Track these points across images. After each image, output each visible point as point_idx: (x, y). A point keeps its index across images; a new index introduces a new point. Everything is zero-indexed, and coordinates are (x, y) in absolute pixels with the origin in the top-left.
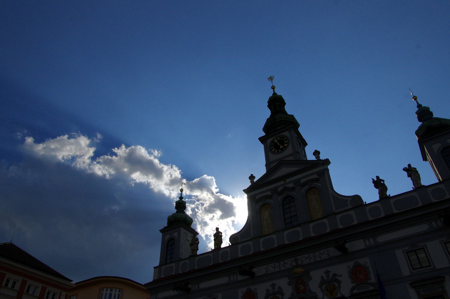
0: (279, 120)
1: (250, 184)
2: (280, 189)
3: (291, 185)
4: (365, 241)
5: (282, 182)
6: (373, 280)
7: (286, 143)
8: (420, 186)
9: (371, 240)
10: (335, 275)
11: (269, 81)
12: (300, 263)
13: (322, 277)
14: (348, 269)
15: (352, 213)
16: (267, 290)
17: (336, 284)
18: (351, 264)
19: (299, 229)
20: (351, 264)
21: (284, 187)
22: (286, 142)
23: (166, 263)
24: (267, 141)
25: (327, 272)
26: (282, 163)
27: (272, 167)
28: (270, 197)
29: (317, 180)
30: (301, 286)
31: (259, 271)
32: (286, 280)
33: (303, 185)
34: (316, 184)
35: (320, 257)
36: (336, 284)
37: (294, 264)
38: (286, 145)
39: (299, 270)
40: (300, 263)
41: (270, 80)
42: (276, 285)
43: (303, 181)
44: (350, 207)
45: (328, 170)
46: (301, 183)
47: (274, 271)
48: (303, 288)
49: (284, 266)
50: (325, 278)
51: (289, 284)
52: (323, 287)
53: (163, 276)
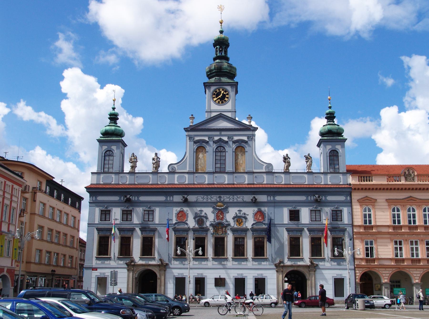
0: (224, 71)
2: (216, 138)
3: (225, 139)
4: (268, 197)
5: (218, 133)
6: (266, 222)
7: (227, 98)
8: (310, 171)
9: (272, 197)
10: (245, 214)
11: (219, 10)
12: (222, 200)
13: (236, 213)
14: (254, 211)
16: (196, 213)
18: (256, 209)
20: (256, 209)
21: (220, 138)
22: (227, 96)
24: (210, 88)
25: (240, 211)
26: (221, 116)
27: (212, 116)
28: (207, 142)
29: (246, 142)
30: (220, 215)
31: (192, 198)
32: (211, 209)
34: (244, 144)
35: (237, 199)
36: (244, 220)
37: (218, 200)
38: (226, 99)
40: (222, 200)
41: (220, 9)
43: (236, 138)
45: (254, 135)
46: (233, 140)
47: (202, 201)
48: (221, 217)
49: (211, 199)
50: (238, 214)
51: (213, 212)
52: (235, 219)
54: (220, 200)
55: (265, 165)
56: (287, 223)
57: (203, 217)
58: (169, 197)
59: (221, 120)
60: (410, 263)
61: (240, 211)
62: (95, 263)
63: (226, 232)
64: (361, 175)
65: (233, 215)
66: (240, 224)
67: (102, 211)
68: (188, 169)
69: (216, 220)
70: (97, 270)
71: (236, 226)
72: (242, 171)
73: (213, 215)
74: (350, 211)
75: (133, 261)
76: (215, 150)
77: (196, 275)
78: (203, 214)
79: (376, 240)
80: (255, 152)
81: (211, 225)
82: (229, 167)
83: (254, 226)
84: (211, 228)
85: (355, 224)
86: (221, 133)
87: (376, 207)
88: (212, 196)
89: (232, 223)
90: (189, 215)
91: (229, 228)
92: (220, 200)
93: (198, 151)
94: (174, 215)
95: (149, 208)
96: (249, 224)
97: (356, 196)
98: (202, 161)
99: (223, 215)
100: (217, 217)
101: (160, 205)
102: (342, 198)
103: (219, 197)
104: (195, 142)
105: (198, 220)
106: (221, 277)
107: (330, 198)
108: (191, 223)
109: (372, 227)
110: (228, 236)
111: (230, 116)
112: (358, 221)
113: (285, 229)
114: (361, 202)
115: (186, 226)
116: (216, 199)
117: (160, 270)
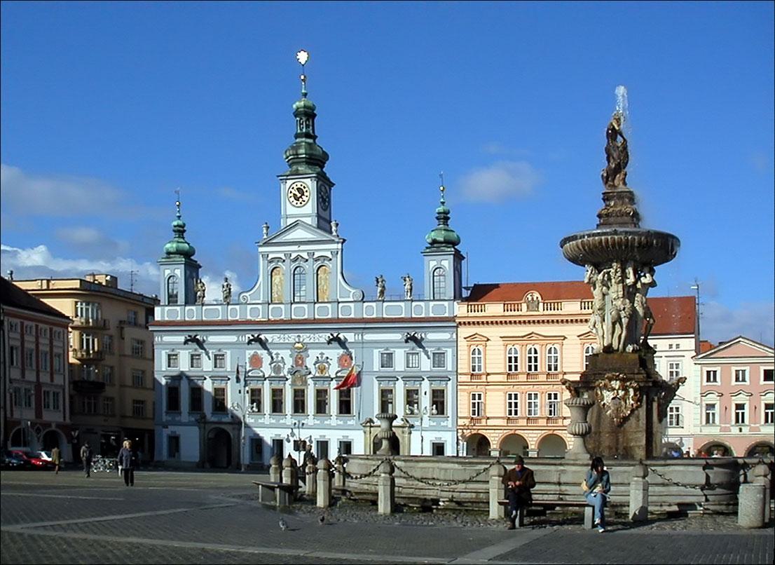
2: (294, 255)
3: (305, 255)
9: (360, 335)
10: (327, 358)
12: (301, 340)
13: (318, 358)
15: (352, 305)
17: (327, 366)
19: (305, 306)
23: (169, 305)
27: (288, 224)
32: (289, 352)
37: (297, 340)
39: (300, 345)
42: (279, 354)
43: (317, 254)
46: (315, 257)
48: (300, 362)
50: (320, 358)
51: (291, 356)
52: (317, 365)
53: (166, 319)
54: (299, 339)
56: (378, 370)
58: (240, 337)
59: (299, 230)
60: (523, 422)
61: (322, 354)
62: (165, 418)
63: (306, 382)
64: (470, 303)
65: (315, 359)
67: (169, 356)
68: (262, 299)
69: (294, 366)
70: (167, 428)
71: (317, 375)
72: (326, 300)
73: (291, 359)
75: (204, 417)
77: (274, 436)
78: (280, 359)
81: (289, 372)
84: (289, 376)
85: (459, 371)
87: (487, 348)
88: (290, 335)
89: (313, 373)
91: (311, 376)
92: (299, 339)
93: (273, 273)
94: (247, 361)
95: (220, 350)
96: (333, 370)
98: (279, 288)
99: (303, 362)
100: (296, 362)
101: (234, 346)
103: (299, 336)
105: (275, 366)
108: (267, 370)
110: (309, 387)
112: (464, 367)
113: (375, 379)
115: (261, 374)
116: (295, 339)
117: (234, 429)
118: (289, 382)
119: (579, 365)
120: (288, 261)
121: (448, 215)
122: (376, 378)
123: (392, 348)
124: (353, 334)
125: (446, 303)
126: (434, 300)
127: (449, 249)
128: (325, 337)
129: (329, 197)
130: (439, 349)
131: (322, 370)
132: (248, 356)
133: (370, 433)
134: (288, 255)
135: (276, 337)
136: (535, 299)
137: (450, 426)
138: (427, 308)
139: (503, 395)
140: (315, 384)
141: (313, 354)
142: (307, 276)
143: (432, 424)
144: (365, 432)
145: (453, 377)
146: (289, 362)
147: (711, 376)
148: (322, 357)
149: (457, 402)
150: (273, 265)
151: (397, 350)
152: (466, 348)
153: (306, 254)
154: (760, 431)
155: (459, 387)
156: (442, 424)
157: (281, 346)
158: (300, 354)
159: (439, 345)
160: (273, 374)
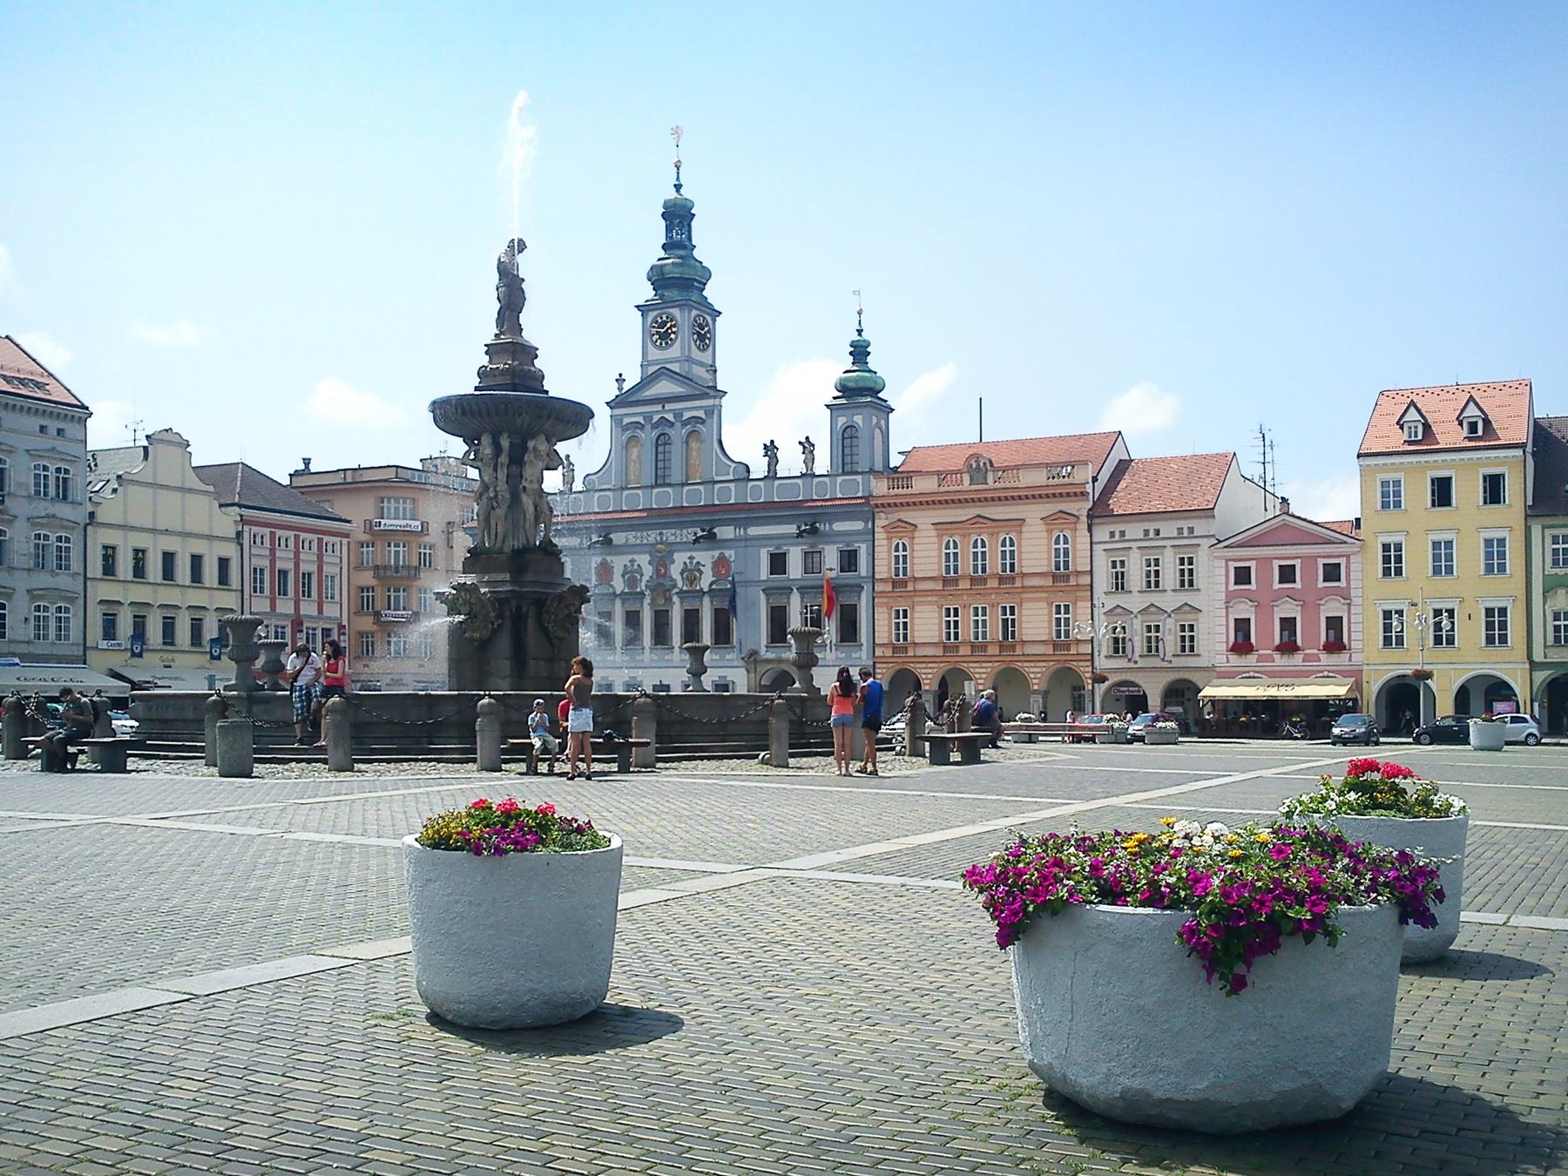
1: (618, 393)
2: (656, 418)
3: (670, 417)
5: (659, 407)
10: (698, 563)
13: (685, 563)
15: (732, 485)
18: (716, 554)
19: (669, 490)
20: (716, 554)
25: (691, 558)
26: (664, 372)
29: (703, 422)
31: (618, 538)
32: (647, 557)
33: (685, 423)
43: (687, 415)
44: (731, 477)
46: (684, 418)
48: (663, 571)
51: (650, 563)
54: (661, 539)
55: (733, 465)
57: (636, 571)
61: (691, 558)
66: (691, 583)
69: (655, 577)
71: (685, 588)
73: (651, 568)
74: (871, 552)
76: (657, 442)
78: (635, 567)
79: (913, 608)
80: (720, 442)
82: (676, 477)
83: (714, 587)
85: (877, 576)
86: (663, 407)
87: (916, 540)
89: (680, 584)
90: (615, 570)
92: (661, 539)
93: (630, 445)
94: (593, 571)
96: (705, 582)
97: (881, 521)
99: (666, 568)
100: (657, 571)
102: (858, 525)
103: (661, 533)
104: (625, 428)
106: (664, 683)
107: (839, 526)
108: (619, 585)
109: (904, 583)
110: (674, 607)
111: (678, 371)
114: (890, 529)
115: (611, 590)
118: (647, 600)
119: (1045, 562)
120: (648, 427)
121: (868, 349)
122: (763, 590)
123: (785, 545)
124: (733, 527)
125: (859, 478)
126: (844, 473)
127: (864, 400)
128: (688, 534)
129: (712, 332)
130: (848, 546)
131: (692, 580)
132: (594, 565)
133: (755, 672)
134: (648, 417)
135: (630, 537)
136: (981, 464)
137: (864, 657)
138: (834, 485)
139: (937, 609)
140: (682, 603)
141: (680, 558)
142: (673, 448)
143: (840, 655)
144: (748, 671)
145: (867, 587)
146: (648, 571)
147: (1242, 576)
148: (691, 563)
149: (878, 624)
150: (628, 433)
151: (791, 549)
152: (885, 542)
153: (672, 415)
154: (1320, 661)
155: (876, 600)
156: (854, 655)
157: (636, 549)
158: (662, 562)
159: (848, 539)
160: (626, 590)
